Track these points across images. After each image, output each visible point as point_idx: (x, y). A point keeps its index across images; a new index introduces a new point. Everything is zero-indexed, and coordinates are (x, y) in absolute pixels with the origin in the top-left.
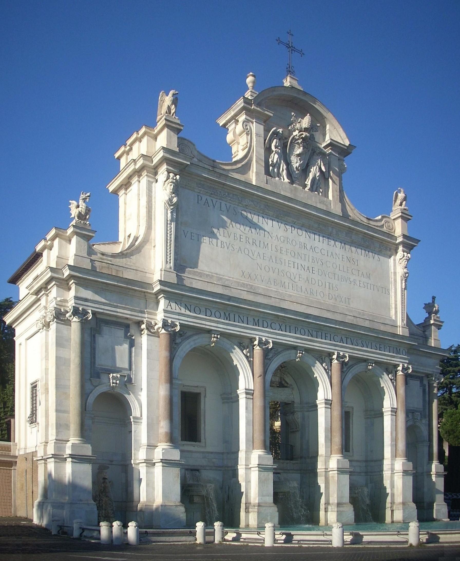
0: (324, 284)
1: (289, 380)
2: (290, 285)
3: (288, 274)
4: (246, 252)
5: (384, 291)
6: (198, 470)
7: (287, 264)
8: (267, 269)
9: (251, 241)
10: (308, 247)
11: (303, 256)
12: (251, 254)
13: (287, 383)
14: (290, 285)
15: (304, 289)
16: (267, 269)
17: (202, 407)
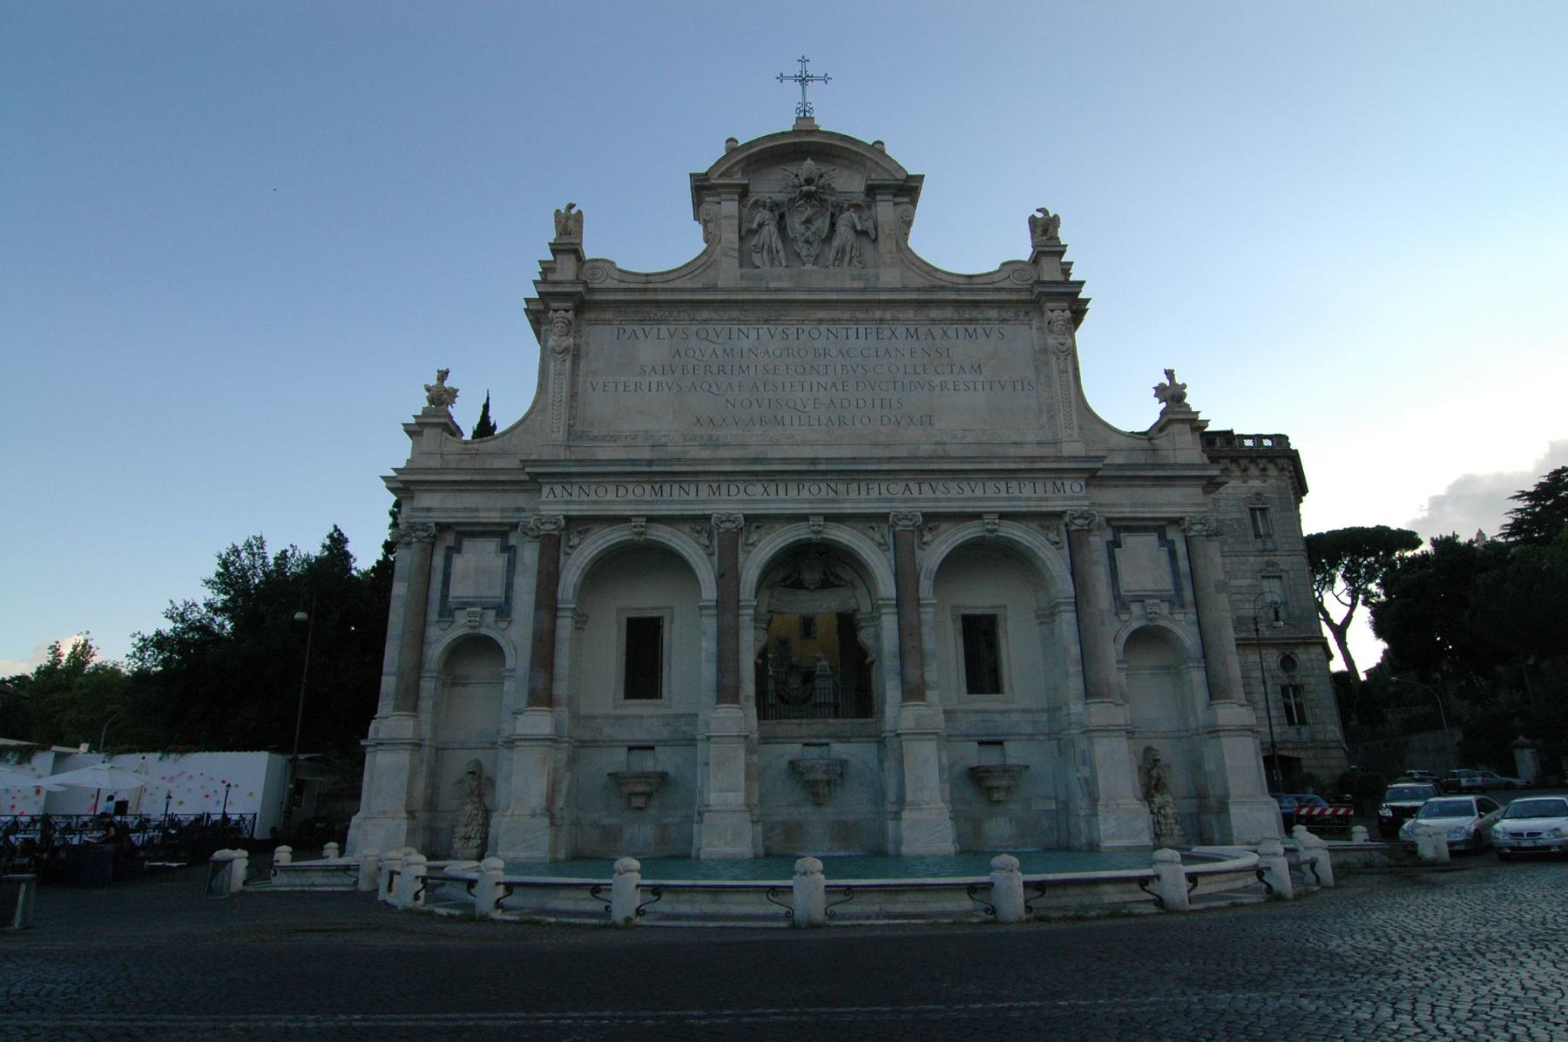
0: (869, 403)
1: (847, 575)
2: (796, 421)
3: (791, 404)
4: (706, 387)
5: (1019, 387)
6: (652, 748)
7: (788, 388)
8: (746, 403)
9: (715, 370)
10: (834, 352)
11: (822, 369)
12: (714, 389)
13: (841, 579)
14: (796, 421)
15: (824, 420)
16: (746, 403)
17: (665, 640)
